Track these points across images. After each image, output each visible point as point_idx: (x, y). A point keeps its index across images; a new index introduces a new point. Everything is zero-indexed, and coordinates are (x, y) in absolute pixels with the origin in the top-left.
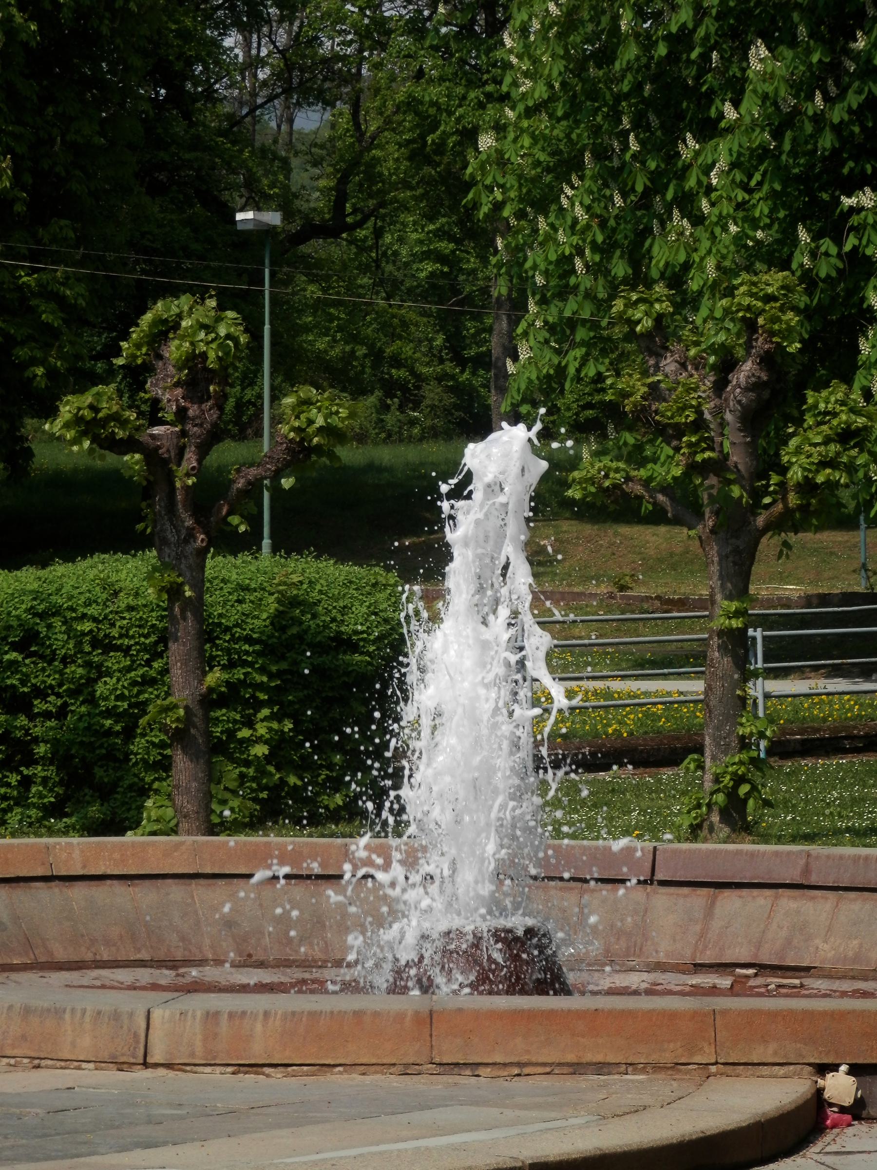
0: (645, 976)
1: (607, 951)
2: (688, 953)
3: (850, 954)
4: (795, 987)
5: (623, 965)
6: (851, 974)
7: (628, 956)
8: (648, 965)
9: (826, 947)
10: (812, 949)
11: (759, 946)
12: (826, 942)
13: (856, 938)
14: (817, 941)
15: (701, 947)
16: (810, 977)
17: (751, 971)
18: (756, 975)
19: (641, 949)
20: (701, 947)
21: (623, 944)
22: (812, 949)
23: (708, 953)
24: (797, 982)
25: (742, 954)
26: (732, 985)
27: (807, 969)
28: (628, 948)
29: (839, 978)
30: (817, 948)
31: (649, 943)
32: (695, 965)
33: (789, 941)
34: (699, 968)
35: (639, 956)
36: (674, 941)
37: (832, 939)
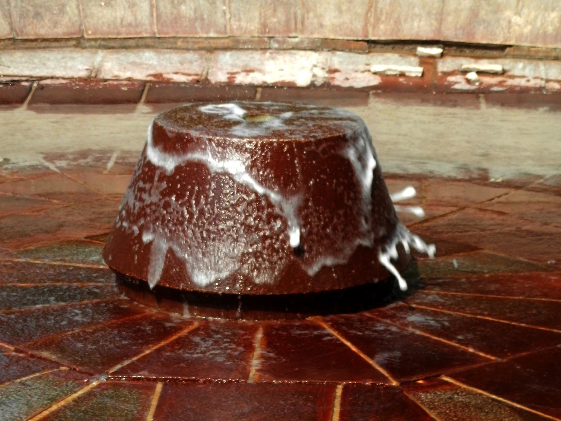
0: (314, 57)
1: (264, 25)
2: (358, 26)
3: (550, 29)
4: (495, 74)
5: (284, 42)
6: (554, 54)
7: (289, 31)
8: (313, 41)
9: (516, 19)
10: (504, 24)
11: (441, 19)
12: (518, 13)
13: (553, 10)
14: (508, 13)
15: (372, 20)
16: (505, 57)
17: (436, 51)
18: (442, 55)
19: (303, 23)
20: (372, 20)
21: (281, 15)
22: (504, 24)
23: (382, 27)
24: (497, 67)
25: (420, 28)
26: (423, 74)
27: (502, 48)
28: (288, 21)
29: (541, 59)
30: (510, 22)
31: (311, 15)
32: (368, 42)
33: (474, 14)
34: (373, 45)
35: (302, 32)
36: (340, 11)
37: (525, 11)
